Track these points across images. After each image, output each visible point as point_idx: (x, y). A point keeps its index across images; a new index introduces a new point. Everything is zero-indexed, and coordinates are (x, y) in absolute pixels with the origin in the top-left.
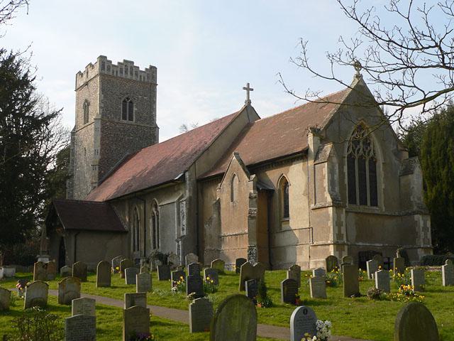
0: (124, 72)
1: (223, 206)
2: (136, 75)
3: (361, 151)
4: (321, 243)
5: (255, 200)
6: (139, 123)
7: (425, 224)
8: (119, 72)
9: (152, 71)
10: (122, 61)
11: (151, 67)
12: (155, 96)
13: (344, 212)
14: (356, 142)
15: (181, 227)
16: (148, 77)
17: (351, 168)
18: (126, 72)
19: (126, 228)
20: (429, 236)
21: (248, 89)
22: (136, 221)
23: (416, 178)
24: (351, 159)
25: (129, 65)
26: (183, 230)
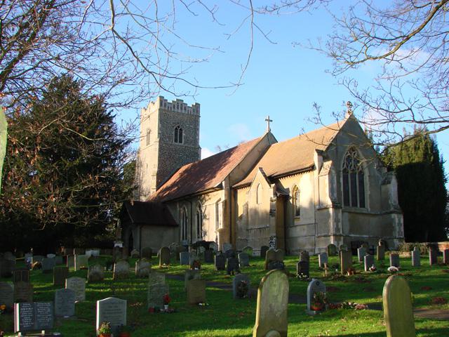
2: (185, 109)
3: (352, 167)
4: (323, 234)
6: (186, 145)
7: (399, 220)
9: (197, 106)
11: (196, 104)
12: (198, 125)
14: (349, 159)
16: (194, 111)
18: (178, 108)
19: (177, 222)
23: (393, 187)
25: (180, 103)
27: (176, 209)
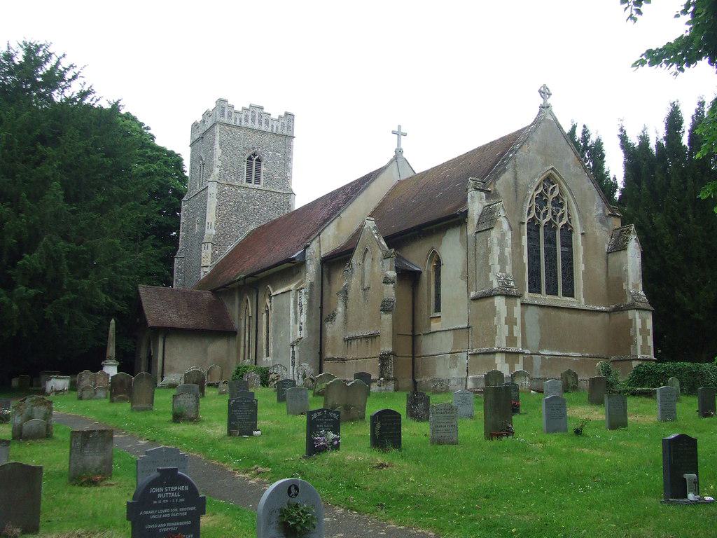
0: (250, 121)
1: (351, 295)
2: (267, 123)
3: (549, 217)
4: (484, 349)
5: (391, 285)
6: (268, 188)
7: (644, 323)
8: (243, 121)
9: (289, 117)
10: (248, 106)
11: (287, 114)
12: (290, 152)
13: (519, 304)
14: (541, 200)
15: (298, 326)
16: (282, 127)
17: (533, 238)
18: (253, 120)
19: (236, 325)
20: (650, 342)
21: (399, 134)
22: (247, 317)
23: (633, 256)
24: (533, 227)
25: (258, 111)
26: (301, 329)
27: (233, 303)
